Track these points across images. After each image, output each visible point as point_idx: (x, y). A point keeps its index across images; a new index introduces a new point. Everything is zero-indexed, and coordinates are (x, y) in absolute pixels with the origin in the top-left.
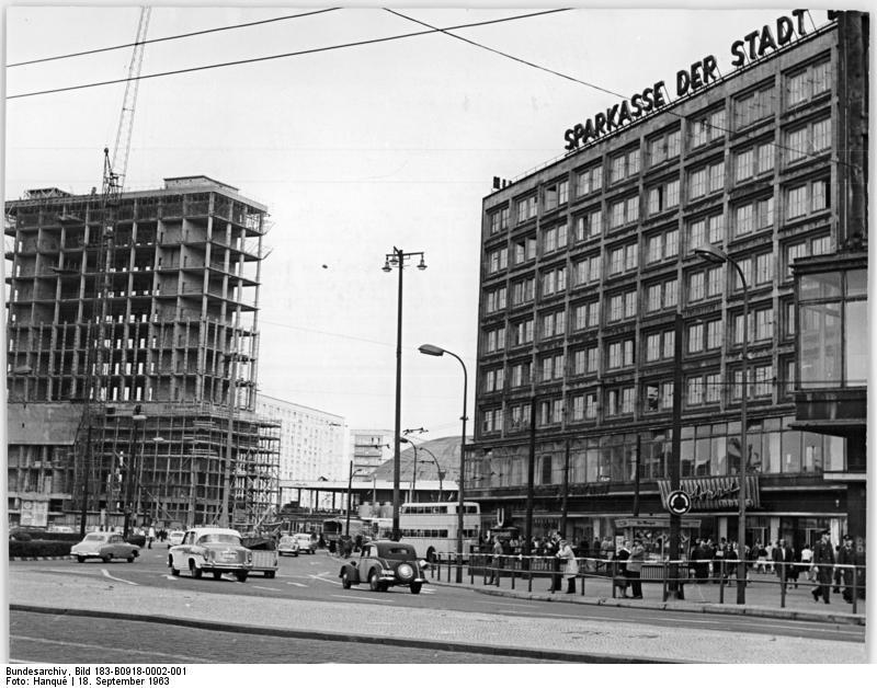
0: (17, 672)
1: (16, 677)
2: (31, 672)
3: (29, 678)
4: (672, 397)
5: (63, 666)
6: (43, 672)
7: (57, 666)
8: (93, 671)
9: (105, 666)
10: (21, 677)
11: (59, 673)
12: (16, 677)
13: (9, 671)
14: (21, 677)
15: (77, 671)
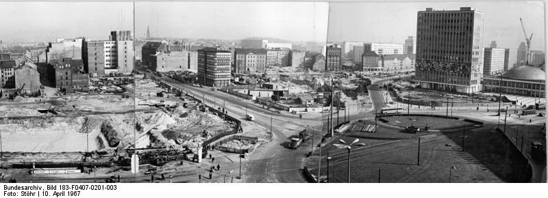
0: (11, 188)
1: (10, 191)
2: (19, 188)
3: (19, 192)
4: (487, 171)
5: (40, 185)
6: (27, 188)
7: (36, 184)
8: (58, 187)
9: (65, 184)
10: (13, 191)
11: (37, 189)
12: (10, 191)
13: (5, 187)
14: (13, 191)
15: (48, 188)
